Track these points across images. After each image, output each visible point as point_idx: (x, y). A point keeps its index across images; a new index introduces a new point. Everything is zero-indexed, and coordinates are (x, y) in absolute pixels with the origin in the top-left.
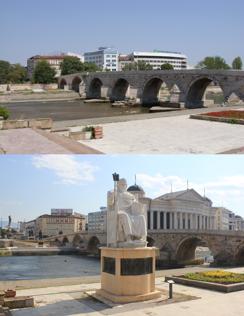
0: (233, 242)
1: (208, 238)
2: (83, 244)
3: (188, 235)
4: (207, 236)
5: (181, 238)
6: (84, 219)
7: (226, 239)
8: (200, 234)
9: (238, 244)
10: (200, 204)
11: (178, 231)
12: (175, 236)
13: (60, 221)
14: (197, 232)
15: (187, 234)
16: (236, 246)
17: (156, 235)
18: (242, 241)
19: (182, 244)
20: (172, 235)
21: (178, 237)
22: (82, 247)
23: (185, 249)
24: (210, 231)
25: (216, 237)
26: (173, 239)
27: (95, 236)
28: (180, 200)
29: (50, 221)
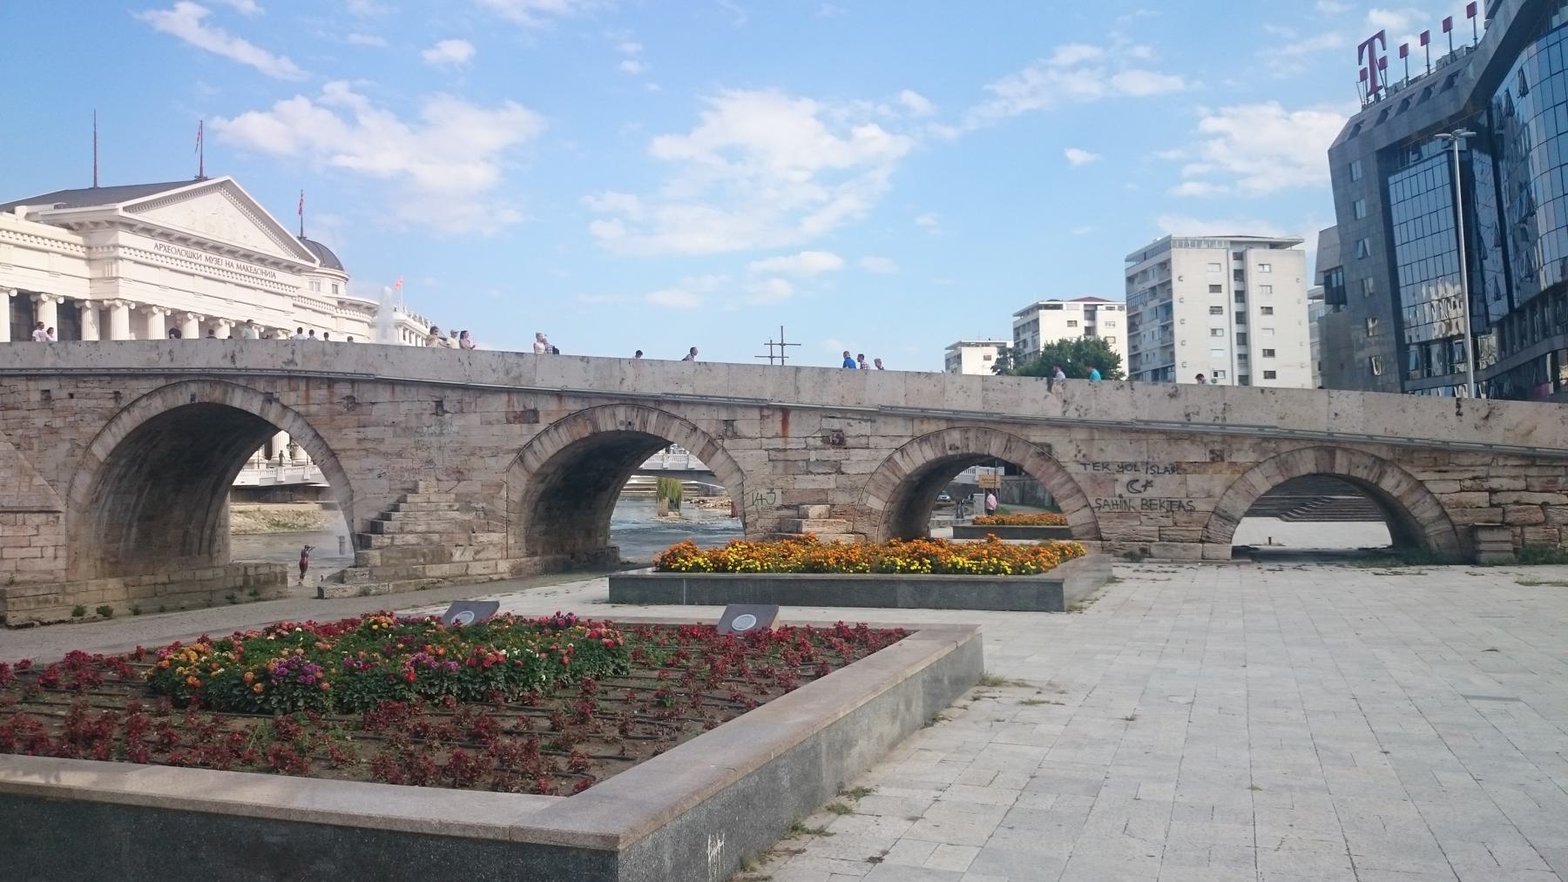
0: (490, 423)
1: (307, 398)
3: (161, 382)
4: (303, 386)
5: (111, 404)
7: (440, 404)
8: (248, 379)
9: (521, 434)
10: (278, 273)
11: (76, 359)
12: (64, 394)
14: (227, 364)
15: (157, 376)
18: (548, 414)
19: (116, 453)
20: (32, 384)
21: (85, 403)
23: (141, 490)
24: (324, 354)
25: (366, 394)
26: (40, 420)
28: (148, 230)
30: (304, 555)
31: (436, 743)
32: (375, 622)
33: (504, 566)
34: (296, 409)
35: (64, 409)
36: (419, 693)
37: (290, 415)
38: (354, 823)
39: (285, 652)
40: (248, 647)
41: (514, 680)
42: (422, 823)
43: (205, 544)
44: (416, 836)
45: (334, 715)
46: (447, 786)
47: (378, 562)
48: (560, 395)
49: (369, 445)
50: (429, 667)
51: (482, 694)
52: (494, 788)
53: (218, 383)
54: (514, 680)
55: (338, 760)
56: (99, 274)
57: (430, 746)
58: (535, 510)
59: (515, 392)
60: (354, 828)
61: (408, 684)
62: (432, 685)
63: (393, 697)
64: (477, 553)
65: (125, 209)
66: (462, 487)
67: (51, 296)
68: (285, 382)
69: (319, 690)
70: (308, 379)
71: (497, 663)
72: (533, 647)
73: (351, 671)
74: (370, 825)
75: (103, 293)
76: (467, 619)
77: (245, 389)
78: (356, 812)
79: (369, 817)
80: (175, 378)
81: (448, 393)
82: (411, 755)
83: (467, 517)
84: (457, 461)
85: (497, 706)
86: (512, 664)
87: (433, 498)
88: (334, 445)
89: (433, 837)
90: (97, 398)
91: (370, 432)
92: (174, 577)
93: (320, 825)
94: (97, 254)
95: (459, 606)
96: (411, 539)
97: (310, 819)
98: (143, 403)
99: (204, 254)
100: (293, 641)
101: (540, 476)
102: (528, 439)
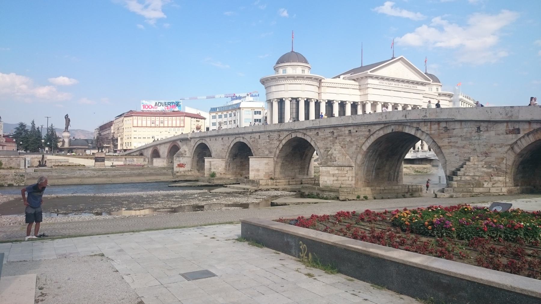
0: (499, 135)
2: (182, 160)
4: (429, 124)
5: (368, 133)
6: (204, 119)
7: (479, 128)
8: (410, 123)
9: (512, 138)
11: (358, 120)
12: (355, 131)
13: (157, 123)
15: (381, 124)
16: (507, 145)
17: (314, 132)
18: (524, 130)
19: (369, 149)
22: (180, 166)
23: (376, 160)
26: (348, 139)
27: (203, 142)
28: (377, 78)
29: (140, 122)
30: (428, 182)
31: (500, 255)
32: (466, 208)
33: (504, 190)
34: (426, 132)
35: (355, 135)
36: (488, 235)
37: (425, 135)
38: (475, 281)
39: (436, 216)
40: (424, 213)
41: (528, 235)
42: (503, 285)
43: (395, 178)
44: (500, 290)
45: (456, 240)
46: (508, 272)
47: (456, 186)
48: (530, 122)
49: (452, 144)
50: (492, 226)
51: (514, 239)
52: (529, 276)
53: (401, 125)
54: (528, 235)
55: (462, 256)
56: (362, 93)
57: (497, 256)
58: (518, 168)
59: (510, 122)
60: (475, 282)
61: (484, 231)
62: (493, 233)
63: (479, 236)
64: (493, 184)
65: (370, 72)
66: (488, 159)
67: (349, 102)
68: (423, 123)
69: (451, 231)
70: (431, 121)
71: (520, 227)
72: (534, 222)
73: (462, 225)
74: (481, 282)
75: (363, 99)
76: (499, 209)
77: (410, 126)
78: (476, 277)
79: (481, 280)
80: (387, 124)
81: (482, 124)
82: (492, 258)
83: (489, 171)
84: (485, 149)
85: (522, 244)
86: (526, 228)
87: (476, 163)
88: (440, 145)
89: (508, 291)
90: (364, 131)
91: (453, 139)
92: (386, 188)
93: (462, 279)
94: (362, 87)
95: (495, 204)
96: (468, 178)
97: (458, 276)
98: (377, 132)
99: (394, 83)
100: (437, 212)
101: (520, 155)
102: (515, 140)
